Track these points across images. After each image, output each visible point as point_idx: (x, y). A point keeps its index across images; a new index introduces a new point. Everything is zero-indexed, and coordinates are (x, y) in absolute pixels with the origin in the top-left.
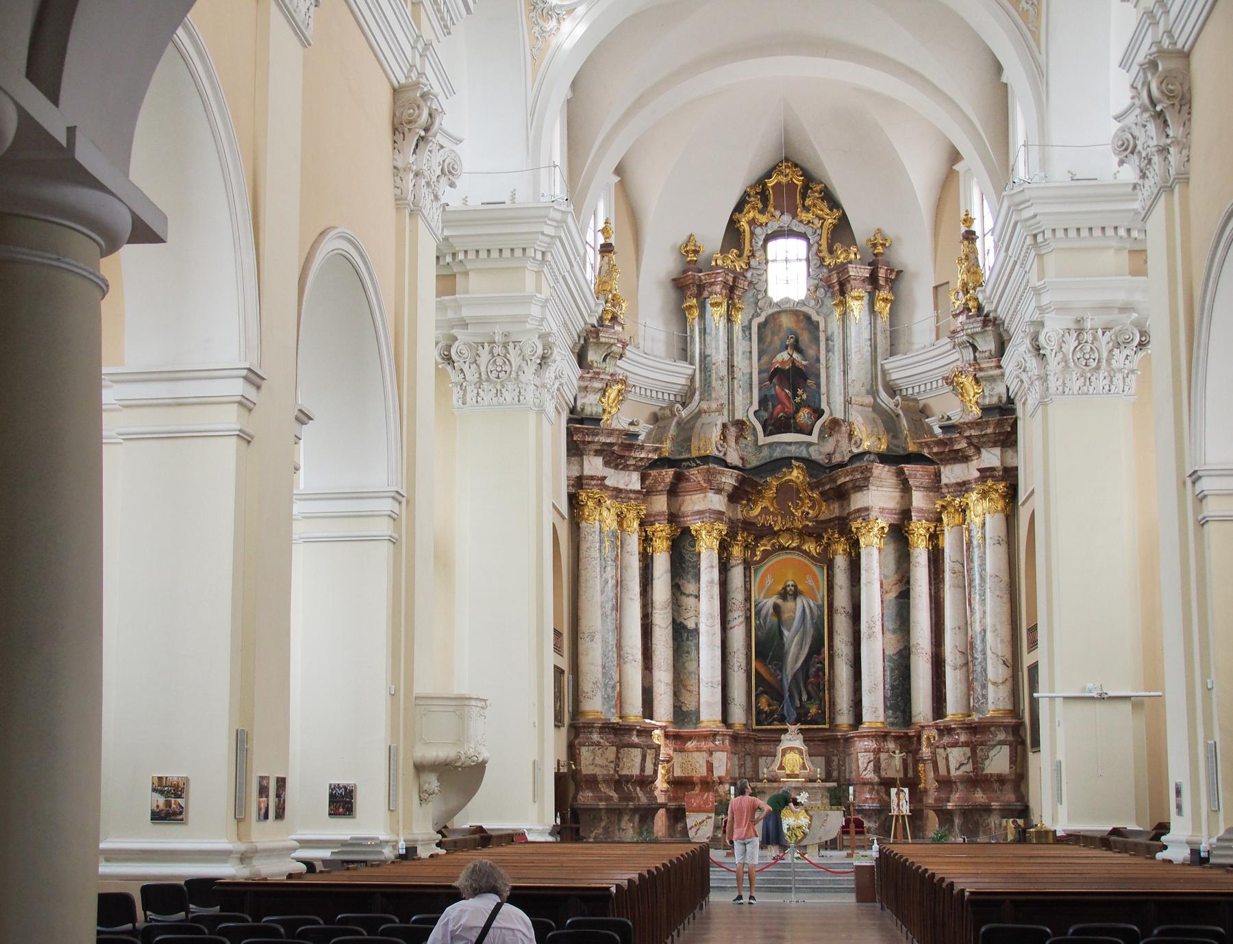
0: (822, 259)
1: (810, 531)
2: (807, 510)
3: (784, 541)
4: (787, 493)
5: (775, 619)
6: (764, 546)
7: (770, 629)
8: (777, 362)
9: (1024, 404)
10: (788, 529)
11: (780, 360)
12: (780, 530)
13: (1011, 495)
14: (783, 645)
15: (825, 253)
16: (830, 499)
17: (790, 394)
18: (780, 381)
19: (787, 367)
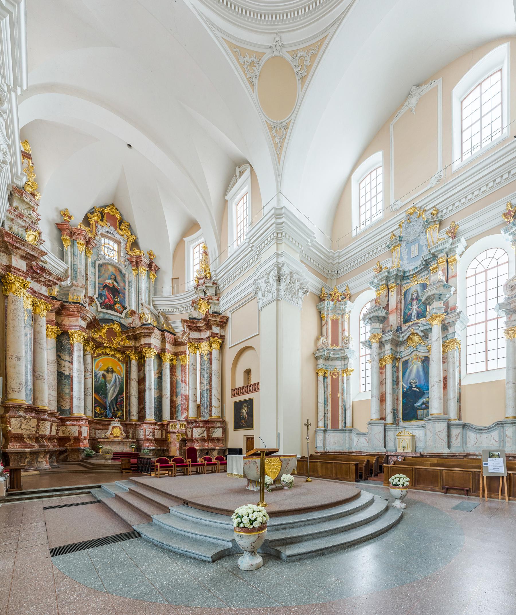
0: (128, 252)
1: (120, 350)
2: (119, 341)
3: (108, 351)
4: (111, 333)
5: (103, 379)
6: (99, 351)
7: (101, 383)
8: (106, 283)
9: (232, 313)
10: (110, 347)
11: (108, 282)
12: (106, 347)
13: (222, 346)
14: (107, 390)
15: (128, 250)
16: (130, 339)
17: (112, 297)
18: (108, 290)
19: (111, 286)
